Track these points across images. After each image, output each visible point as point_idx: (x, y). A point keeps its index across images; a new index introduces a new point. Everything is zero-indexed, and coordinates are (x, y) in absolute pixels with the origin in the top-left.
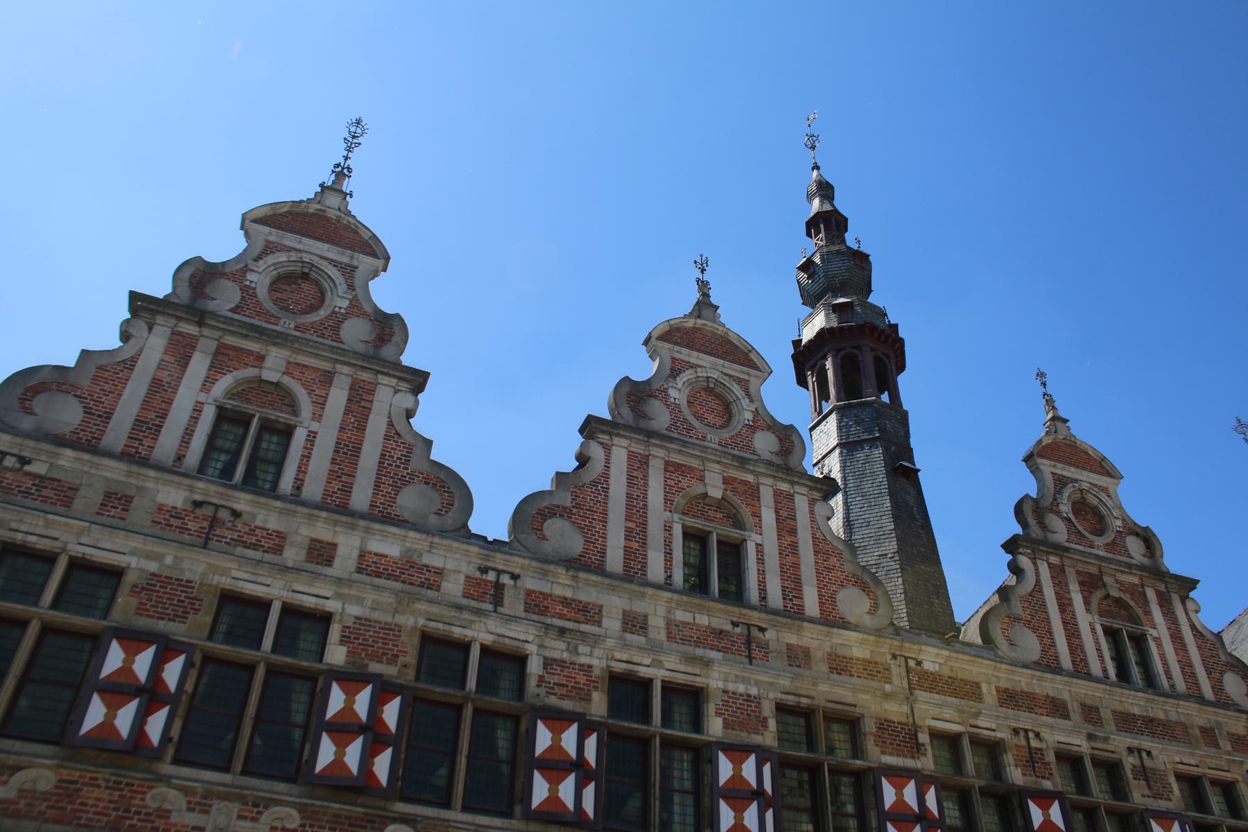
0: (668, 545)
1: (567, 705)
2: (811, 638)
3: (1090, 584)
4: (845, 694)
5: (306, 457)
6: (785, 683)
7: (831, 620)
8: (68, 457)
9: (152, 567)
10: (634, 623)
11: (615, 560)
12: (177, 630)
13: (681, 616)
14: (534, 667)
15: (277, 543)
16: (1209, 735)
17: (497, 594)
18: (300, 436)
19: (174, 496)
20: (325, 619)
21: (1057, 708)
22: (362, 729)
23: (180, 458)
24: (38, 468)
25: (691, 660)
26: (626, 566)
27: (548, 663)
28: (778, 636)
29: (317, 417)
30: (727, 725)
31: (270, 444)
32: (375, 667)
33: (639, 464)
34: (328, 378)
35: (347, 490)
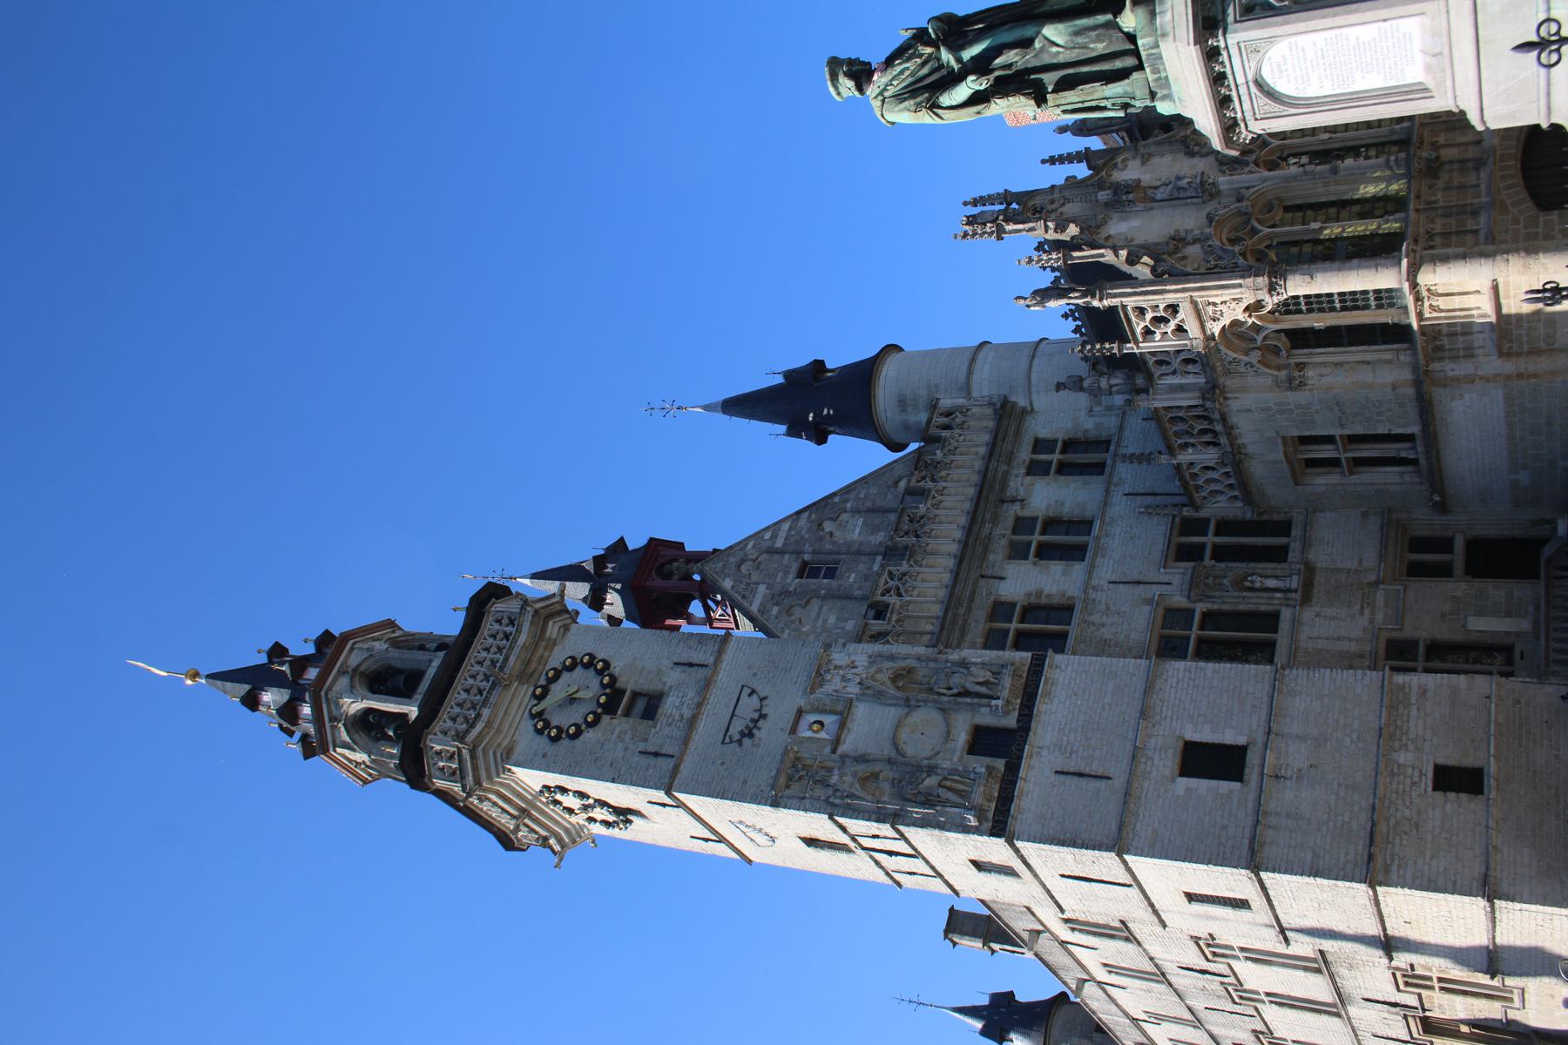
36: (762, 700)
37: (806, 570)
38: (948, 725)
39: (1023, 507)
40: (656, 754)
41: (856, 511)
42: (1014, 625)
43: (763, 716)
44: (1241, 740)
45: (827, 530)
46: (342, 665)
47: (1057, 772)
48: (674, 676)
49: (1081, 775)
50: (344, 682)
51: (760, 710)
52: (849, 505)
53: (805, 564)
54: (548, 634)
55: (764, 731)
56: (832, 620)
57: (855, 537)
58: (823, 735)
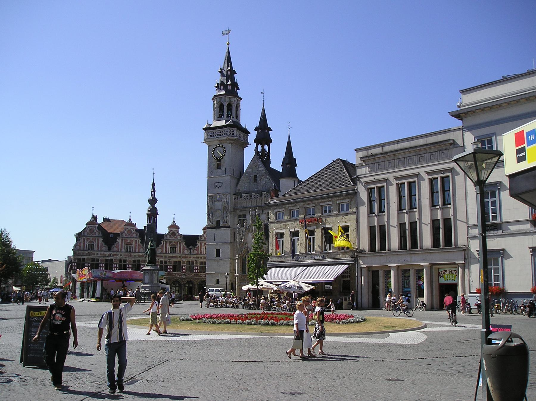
0: (124, 248)
1: (116, 263)
2: (136, 254)
3: (170, 242)
4: (139, 258)
5: (95, 247)
6: (134, 258)
7: (138, 252)
8: (79, 251)
9: (87, 258)
10: (121, 255)
11: (120, 251)
12: (89, 262)
13: (125, 254)
14: (113, 260)
15: (94, 254)
16: (180, 257)
17: (110, 255)
18: (94, 245)
19: (87, 252)
20: (99, 259)
21: (162, 256)
22: (102, 267)
23: (86, 249)
24: (78, 252)
25: (125, 257)
26: (121, 250)
27: (114, 260)
28: (133, 254)
29: (95, 243)
30: (128, 262)
31: (92, 246)
32: (102, 262)
33: (122, 240)
34: (96, 239)
35: (98, 249)
36: (221, 186)
37: (255, 177)
38: (219, 217)
39: (261, 214)
40: (212, 173)
41: (266, 181)
42: (242, 219)
43: (219, 188)
44: (220, 256)
45: (263, 177)
46: (221, 97)
47: (215, 234)
48: (223, 169)
49: (215, 237)
50: (219, 100)
51: (220, 187)
52: (267, 180)
53: (257, 175)
54: (228, 141)
55: (217, 189)
56: (246, 186)
57: (261, 183)
58: (218, 198)
